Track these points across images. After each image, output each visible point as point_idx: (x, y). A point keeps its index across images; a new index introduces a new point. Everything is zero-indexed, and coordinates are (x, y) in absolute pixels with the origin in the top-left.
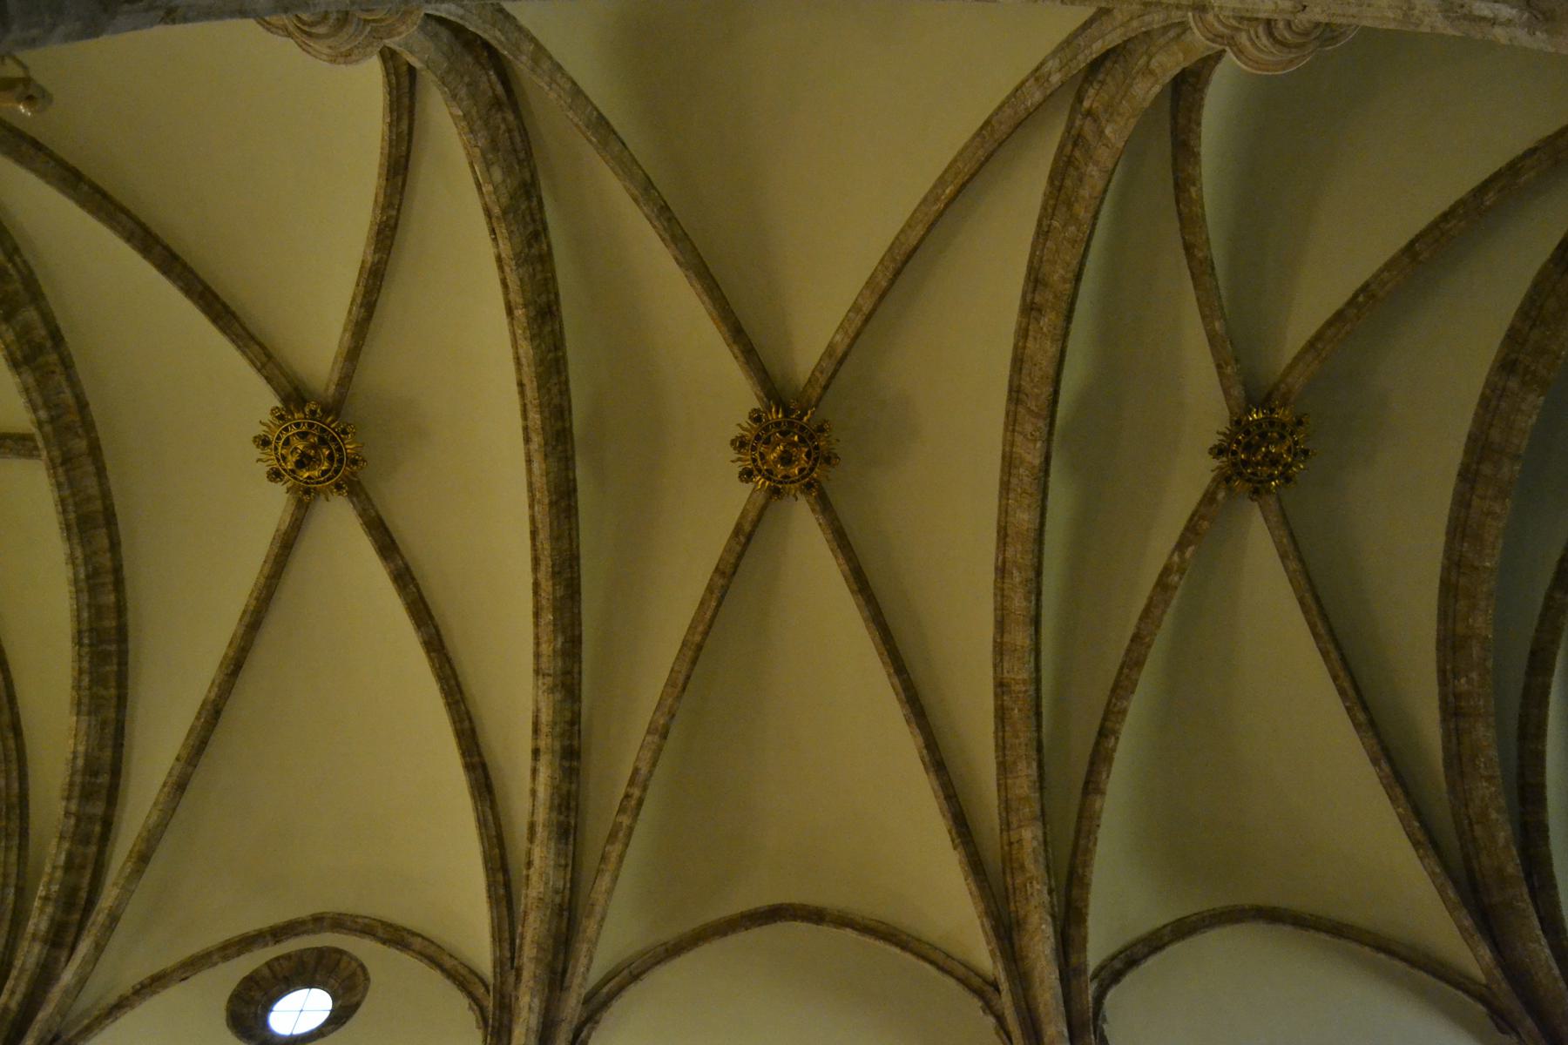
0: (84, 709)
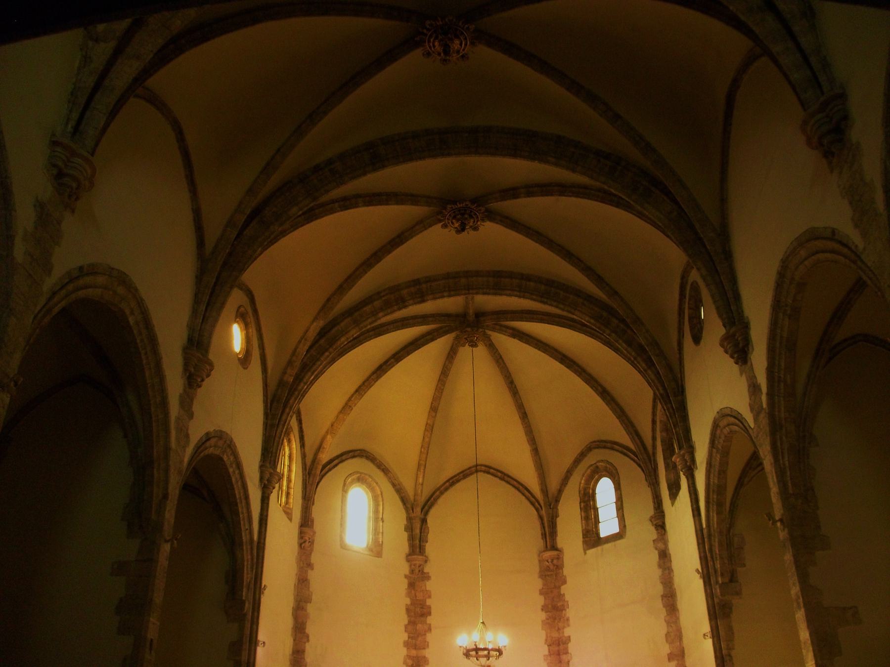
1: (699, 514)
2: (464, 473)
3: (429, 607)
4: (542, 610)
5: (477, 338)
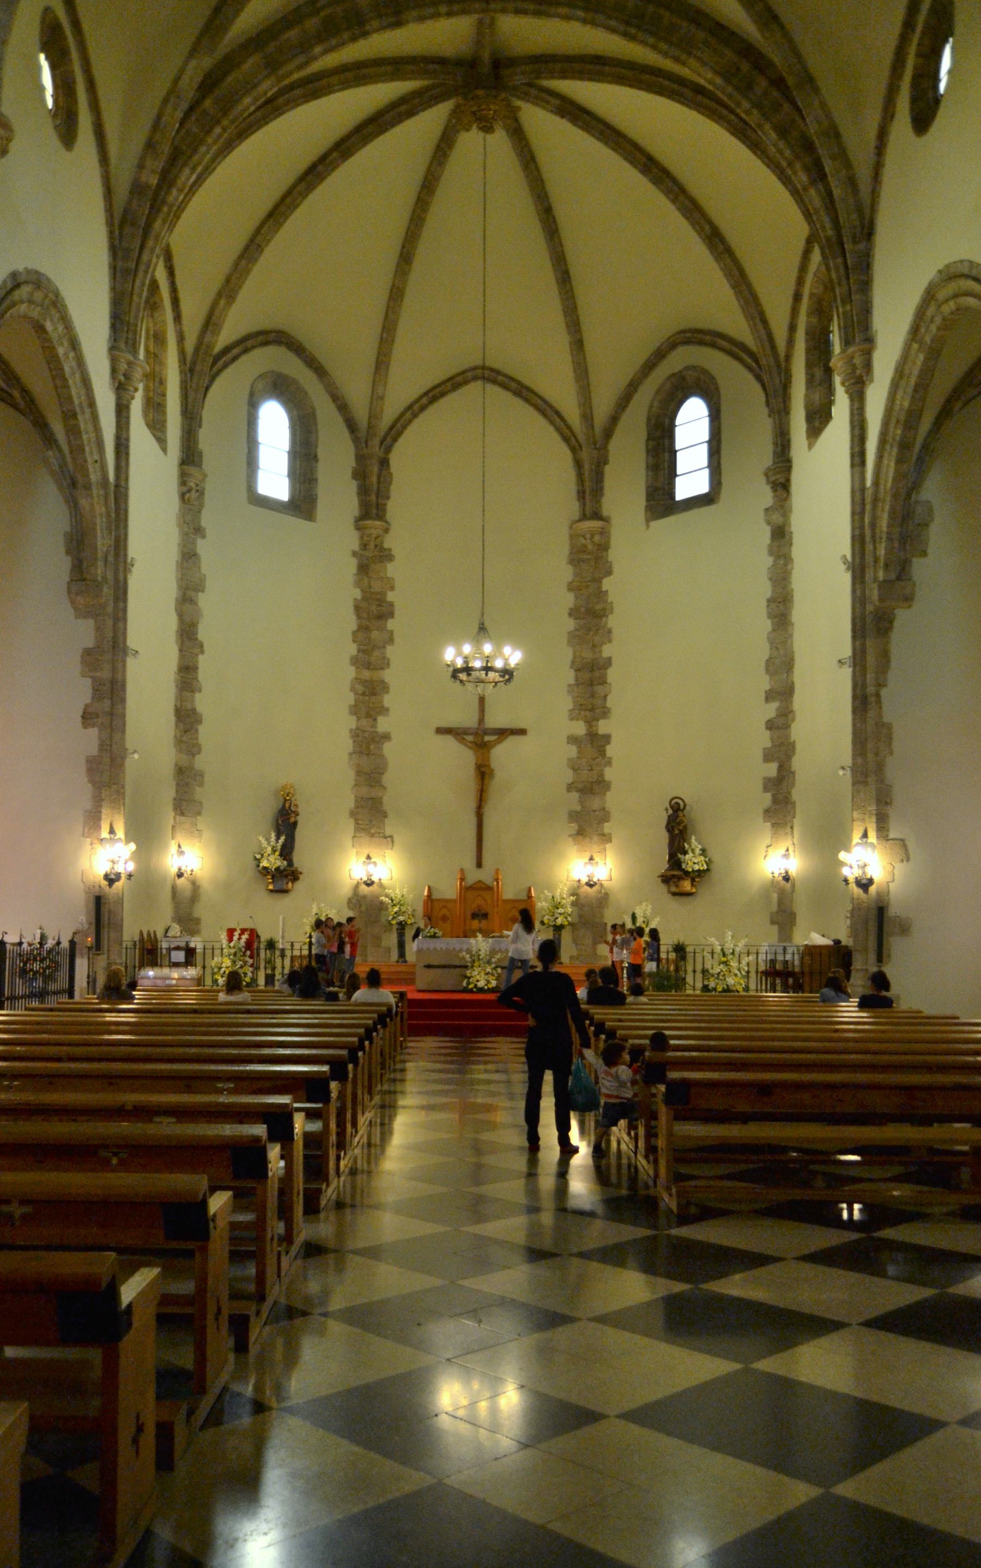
0: (684, 57)
1: (863, 463)
2: (454, 381)
3: (391, 605)
4: (570, 615)
5: (495, 111)
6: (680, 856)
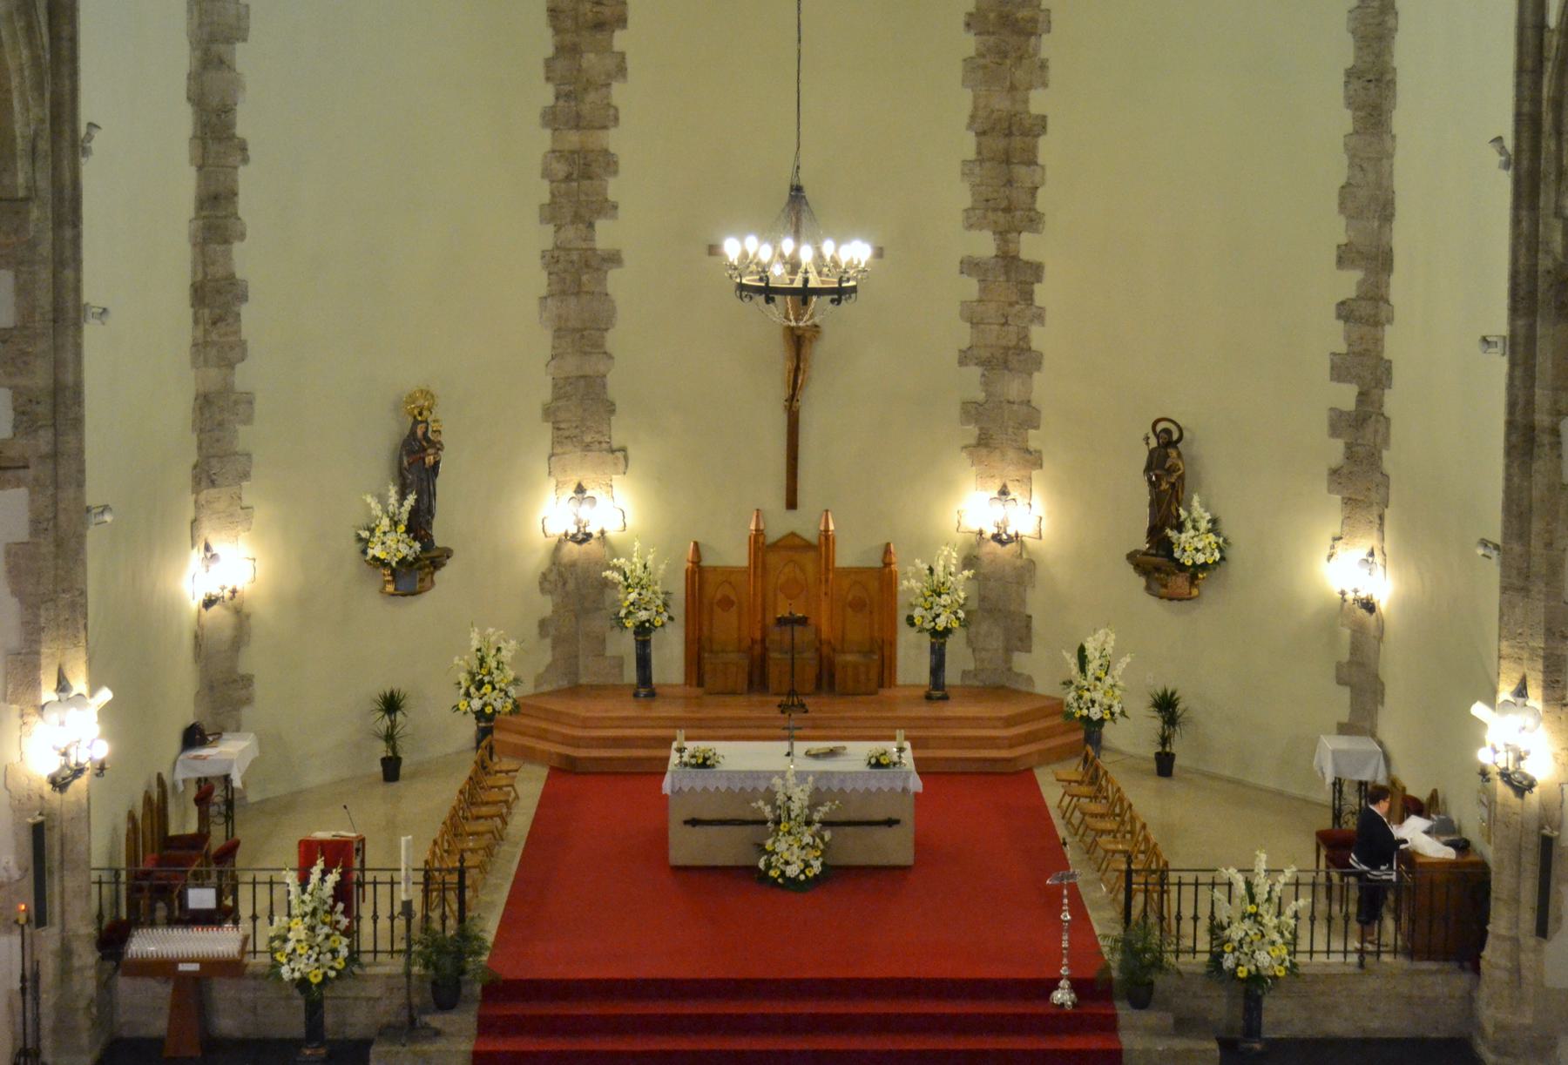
6: (1170, 533)
